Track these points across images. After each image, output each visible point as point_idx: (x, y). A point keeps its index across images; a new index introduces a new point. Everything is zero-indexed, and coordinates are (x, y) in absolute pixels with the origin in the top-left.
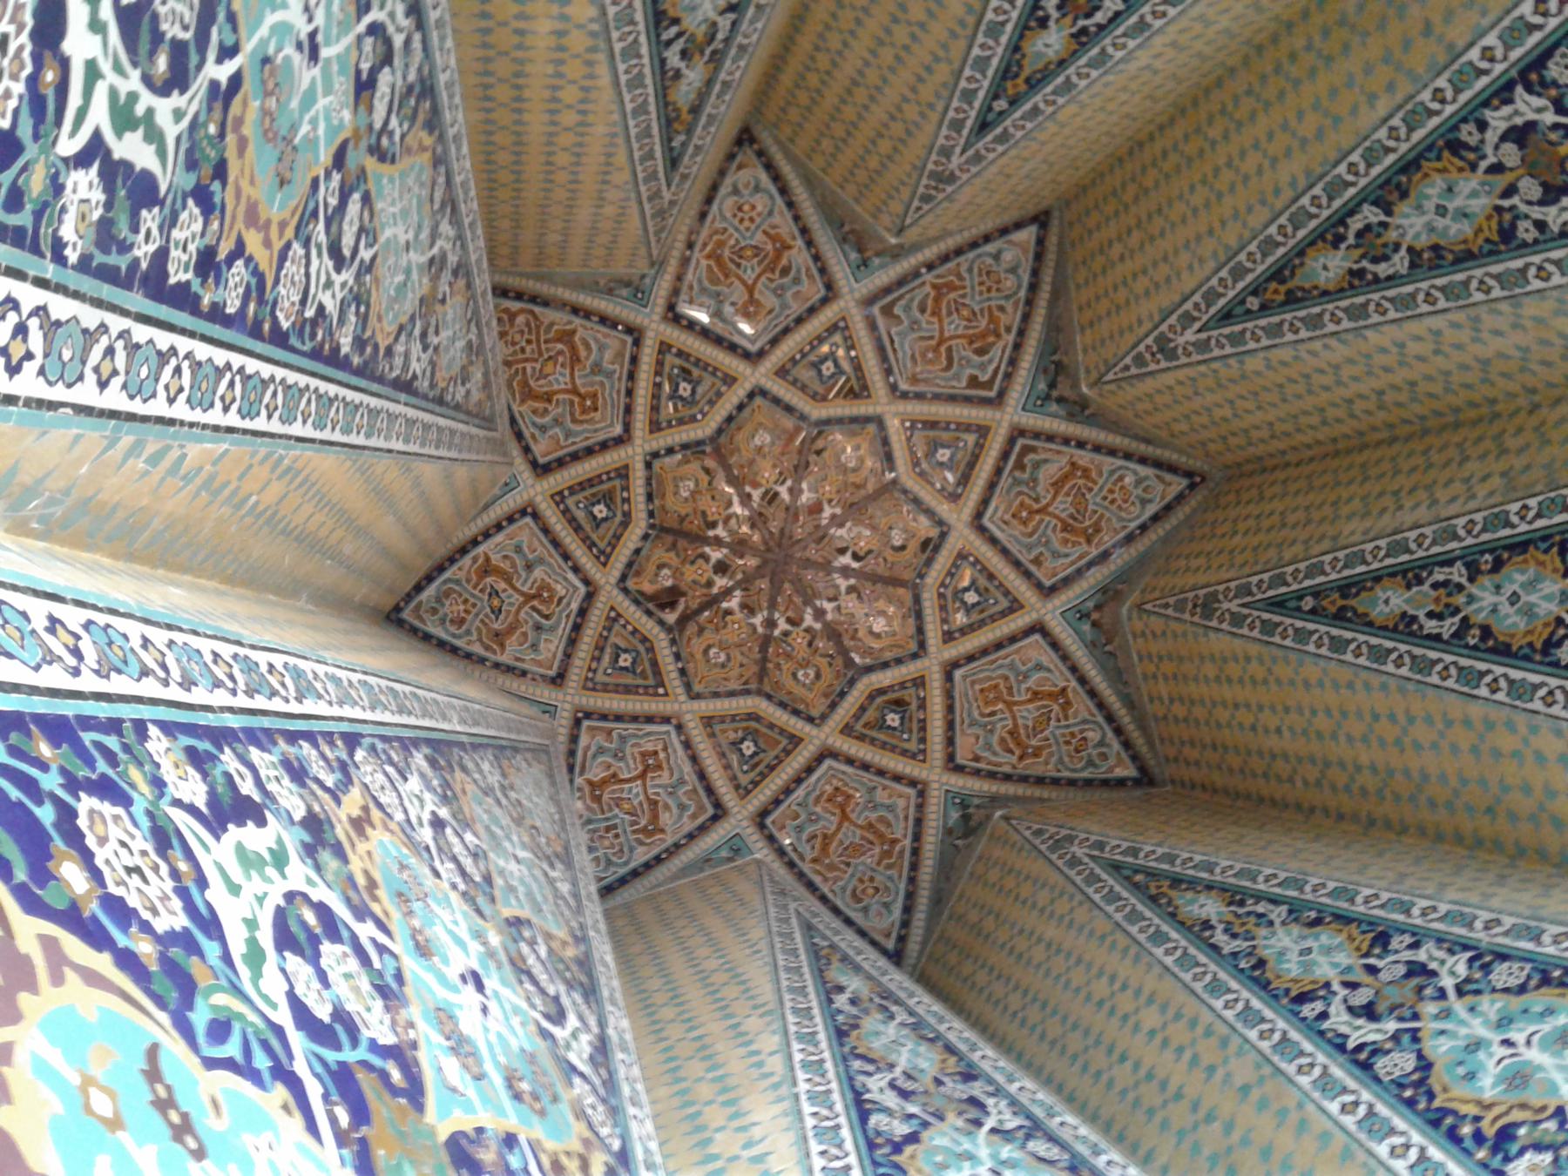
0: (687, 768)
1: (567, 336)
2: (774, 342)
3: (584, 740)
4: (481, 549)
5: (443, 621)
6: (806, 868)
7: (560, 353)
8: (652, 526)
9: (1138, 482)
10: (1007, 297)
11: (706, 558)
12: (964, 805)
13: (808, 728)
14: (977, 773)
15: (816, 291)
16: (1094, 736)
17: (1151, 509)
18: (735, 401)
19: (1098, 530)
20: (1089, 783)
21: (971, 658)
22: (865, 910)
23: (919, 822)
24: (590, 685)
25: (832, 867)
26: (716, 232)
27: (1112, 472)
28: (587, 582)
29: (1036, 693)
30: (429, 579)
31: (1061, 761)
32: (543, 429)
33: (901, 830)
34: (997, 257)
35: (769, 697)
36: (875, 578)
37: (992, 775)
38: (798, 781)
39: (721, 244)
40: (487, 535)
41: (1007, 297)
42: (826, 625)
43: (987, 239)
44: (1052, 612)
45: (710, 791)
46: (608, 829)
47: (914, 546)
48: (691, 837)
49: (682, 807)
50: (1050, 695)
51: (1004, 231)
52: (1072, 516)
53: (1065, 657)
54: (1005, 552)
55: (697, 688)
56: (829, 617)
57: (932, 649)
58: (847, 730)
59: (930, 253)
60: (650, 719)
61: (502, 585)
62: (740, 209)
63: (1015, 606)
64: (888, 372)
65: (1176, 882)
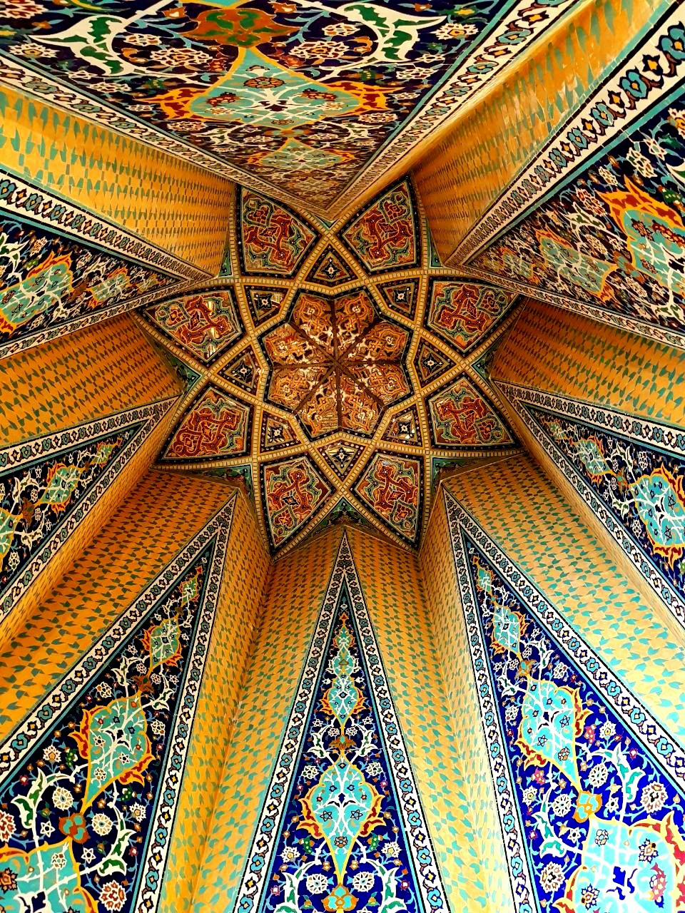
0: (397, 459)
1: (197, 418)
2: (241, 322)
3: (362, 492)
4: (267, 496)
5: (286, 529)
6: (462, 444)
7: (203, 424)
8: (295, 413)
9: (392, 199)
10: (272, 211)
11: (319, 396)
12: (482, 367)
13: (412, 399)
14: (474, 349)
15: (227, 293)
16: (490, 293)
17: (409, 202)
18: (259, 350)
19: (405, 229)
20: (509, 313)
21: (426, 314)
22: (493, 438)
23: (476, 386)
24: (342, 478)
25: (469, 435)
26: (180, 331)
27: (381, 208)
28: (302, 455)
29: (458, 301)
30: (267, 526)
31: (492, 315)
32: (232, 444)
33: (474, 395)
34: (249, 209)
35: (390, 406)
36: (366, 331)
37: (479, 344)
38: (429, 418)
39: (185, 332)
40: (262, 490)
41: (272, 211)
42: (376, 362)
43: (238, 211)
44: (428, 269)
45: (411, 456)
46: (399, 510)
47: (363, 305)
48: (422, 478)
49: (409, 473)
50: (464, 296)
51: (238, 202)
52: (391, 235)
53: (451, 278)
54: (391, 270)
55: (369, 433)
56: (373, 359)
57: (413, 327)
58: (423, 384)
59: (233, 238)
60: (370, 461)
61: (285, 495)
62: (173, 319)
63: (416, 281)
64: (280, 277)
65: (546, 414)
